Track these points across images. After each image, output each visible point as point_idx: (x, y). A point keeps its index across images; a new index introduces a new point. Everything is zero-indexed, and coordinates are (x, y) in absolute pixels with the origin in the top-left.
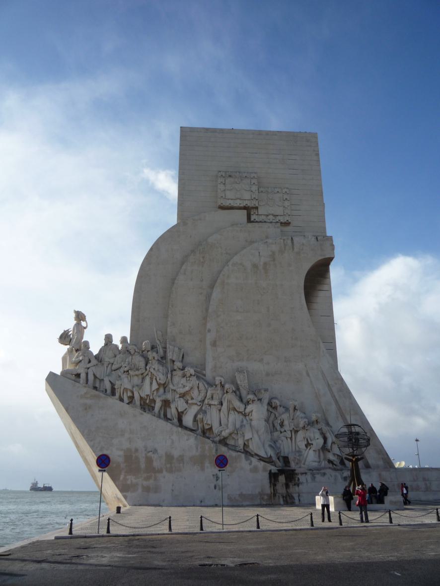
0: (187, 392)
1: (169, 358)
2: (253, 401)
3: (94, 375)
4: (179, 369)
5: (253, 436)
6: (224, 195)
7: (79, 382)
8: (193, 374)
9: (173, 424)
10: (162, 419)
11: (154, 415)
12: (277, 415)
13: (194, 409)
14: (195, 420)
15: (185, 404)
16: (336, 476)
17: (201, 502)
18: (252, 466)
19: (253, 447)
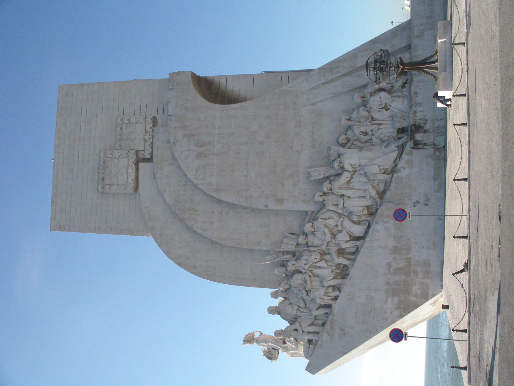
1: (294, 249)
2: (340, 163)
3: (309, 326)
5: (376, 164)
6: (123, 186)
7: (317, 341)
10: (356, 257)
11: (353, 265)
12: (355, 138)
13: (347, 223)
14: (358, 223)
15: (342, 233)
18: (406, 167)
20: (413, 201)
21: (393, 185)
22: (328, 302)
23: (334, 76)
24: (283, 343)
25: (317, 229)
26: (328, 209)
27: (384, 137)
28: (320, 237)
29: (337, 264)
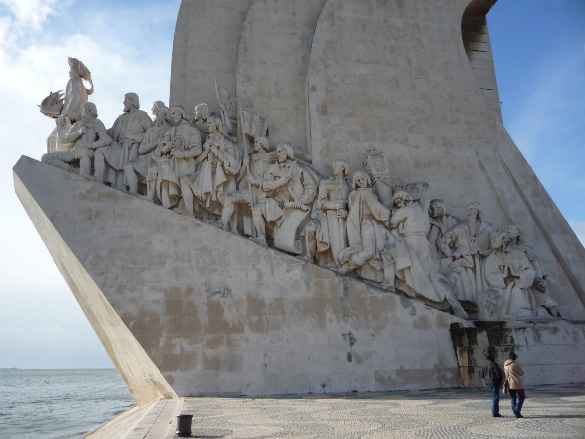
0: (281, 187)
1: (243, 131)
3: (105, 161)
4: (264, 149)
5: (412, 263)
7: (78, 174)
8: (292, 157)
9: (258, 243)
11: (222, 229)
12: (444, 230)
13: (298, 217)
15: (278, 209)
16: (575, 333)
17: (324, 386)
18: (416, 317)
19: (414, 281)
20: (354, 332)
21: (380, 295)
22: (150, 187)
23: (530, 200)
24: (73, 119)
25: (284, 167)
26: (319, 184)
27: (455, 278)
28: (270, 172)
29: (220, 204)
